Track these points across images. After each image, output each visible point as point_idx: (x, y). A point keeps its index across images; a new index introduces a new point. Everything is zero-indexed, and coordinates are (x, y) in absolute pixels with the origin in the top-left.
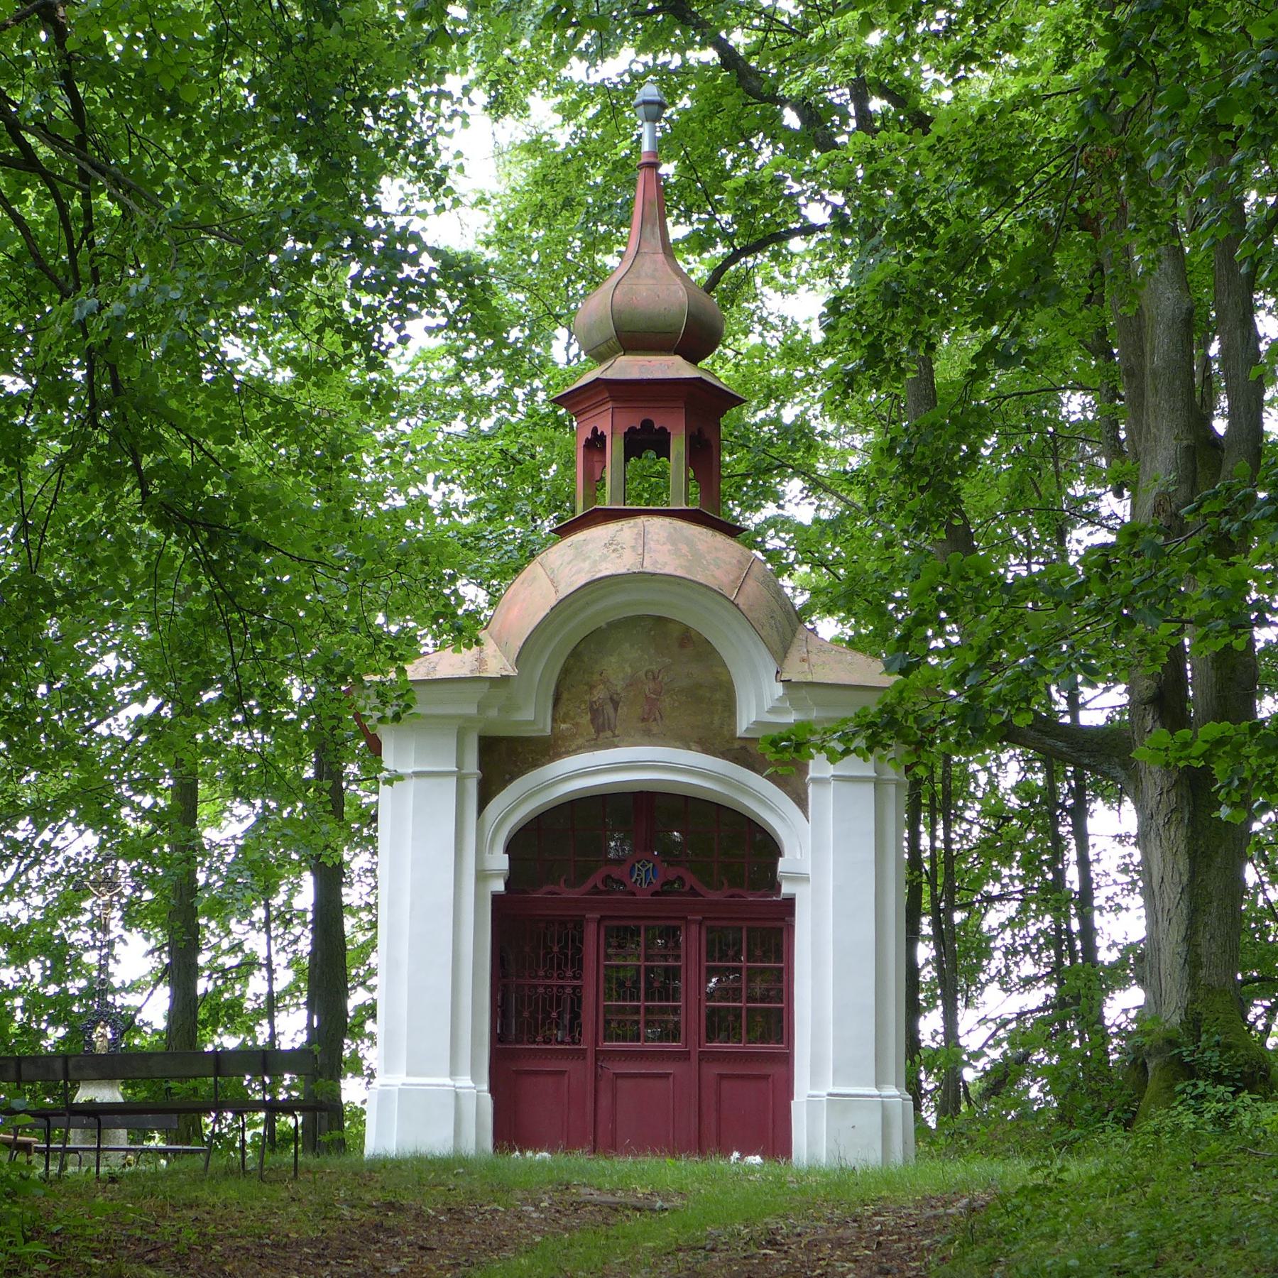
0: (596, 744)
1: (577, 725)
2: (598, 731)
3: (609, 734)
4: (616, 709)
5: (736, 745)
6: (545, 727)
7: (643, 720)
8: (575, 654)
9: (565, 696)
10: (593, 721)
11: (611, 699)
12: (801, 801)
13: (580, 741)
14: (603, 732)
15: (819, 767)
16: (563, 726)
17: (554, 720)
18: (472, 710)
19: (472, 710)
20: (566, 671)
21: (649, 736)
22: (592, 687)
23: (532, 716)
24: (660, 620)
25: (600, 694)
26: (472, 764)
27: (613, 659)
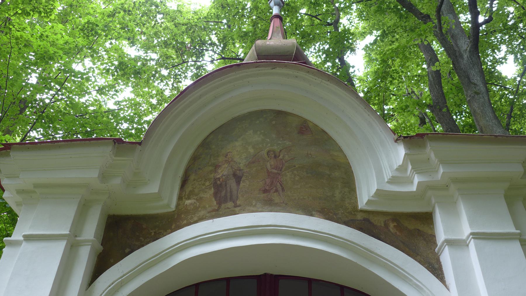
0: (216, 213)
1: (200, 200)
2: (220, 203)
3: (230, 204)
4: (238, 182)
5: (359, 217)
6: (170, 202)
7: (265, 191)
8: (205, 144)
9: (192, 177)
10: (215, 195)
11: (235, 175)
12: (437, 271)
13: (202, 213)
14: (225, 201)
16: (188, 202)
17: (180, 198)
18: (91, 175)
19: (91, 175)
20: (195, 158)
21: (270, 205)
22: (217, 167)
23: (157, 191)
24: (279, 114)
25: (224, 171)
26: (91, 231)
27: (237, 144)
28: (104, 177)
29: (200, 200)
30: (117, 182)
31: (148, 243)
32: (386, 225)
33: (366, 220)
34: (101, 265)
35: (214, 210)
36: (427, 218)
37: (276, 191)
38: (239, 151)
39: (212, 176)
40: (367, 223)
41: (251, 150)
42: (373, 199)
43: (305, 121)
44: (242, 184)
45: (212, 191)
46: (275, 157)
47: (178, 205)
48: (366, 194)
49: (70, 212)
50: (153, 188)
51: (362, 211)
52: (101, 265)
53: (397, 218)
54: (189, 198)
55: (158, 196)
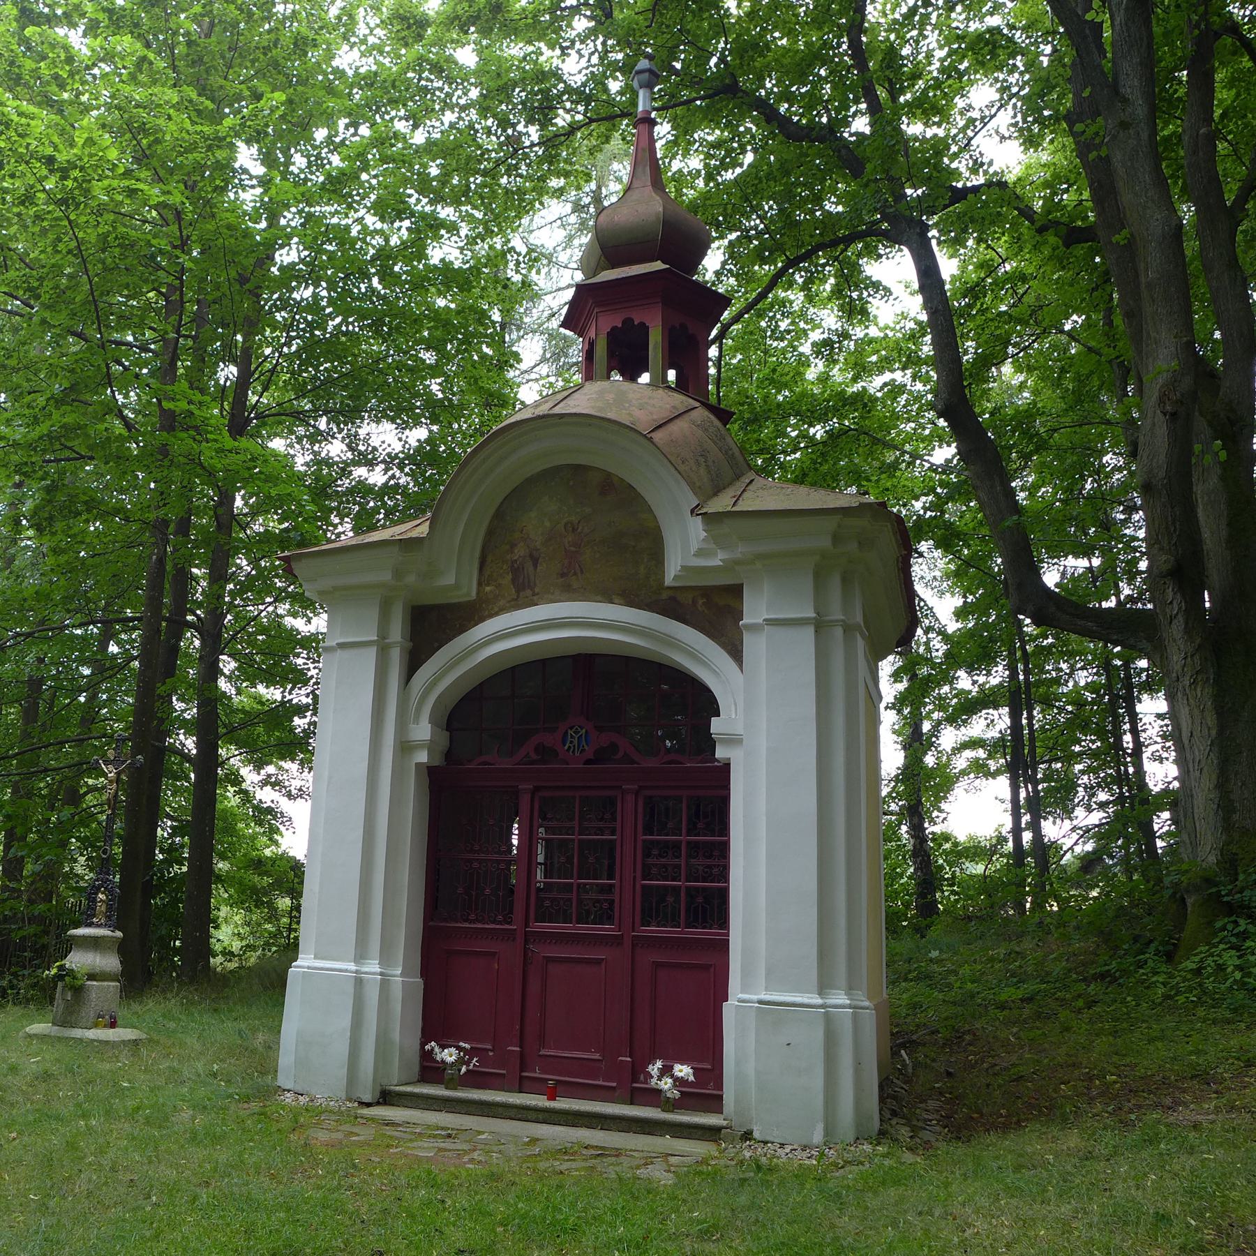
0: (517, 604)
1: (499, 586)
2: (518, 592)
3: (529, 592)
4: (535, 566)
5: (665, 595)
6: (469, 591)
7: (563, 575)
8: (499, 515)
9: (489, 559)
10: (513, 580)
11: (531, 556)
12: (736, 654)
13: (502, 603)
14: (524, 592)
15: (755, 610)
16: (488, 589)
17: (480, 584)
18: (386, 576)
19: (386, 576)
20: (490, 533)
21: (569, 592)
22: (513, 546)
23: (455, 580)
24: (579, 469)
25: (520, 551)
26: (397, 633)
27: (533, 514)
28: (398, 574)
29: (499, 586)
30: (411, 579)
31: (455, 637)
32: (694, 602)
33: (673, 599)
34: (413, 664)
35: (513, 600)
36: (736, 591)
37: (575, 574)
38: (536, 523)
39: (508, 557)
40: (673, 604)
41: (547, 524)
42: (705, 546)
43: (609, 475)
44: (539, 568)
45: (510, 577)
46: (574, 530)
47: (478, 593)
48: (672, 571)
49: (373, 614)
50: (449, 580)
51: (669, 588)
52: (413, 664)
53: (707, 592)
54: (488, 585)
55: (457, 586)
